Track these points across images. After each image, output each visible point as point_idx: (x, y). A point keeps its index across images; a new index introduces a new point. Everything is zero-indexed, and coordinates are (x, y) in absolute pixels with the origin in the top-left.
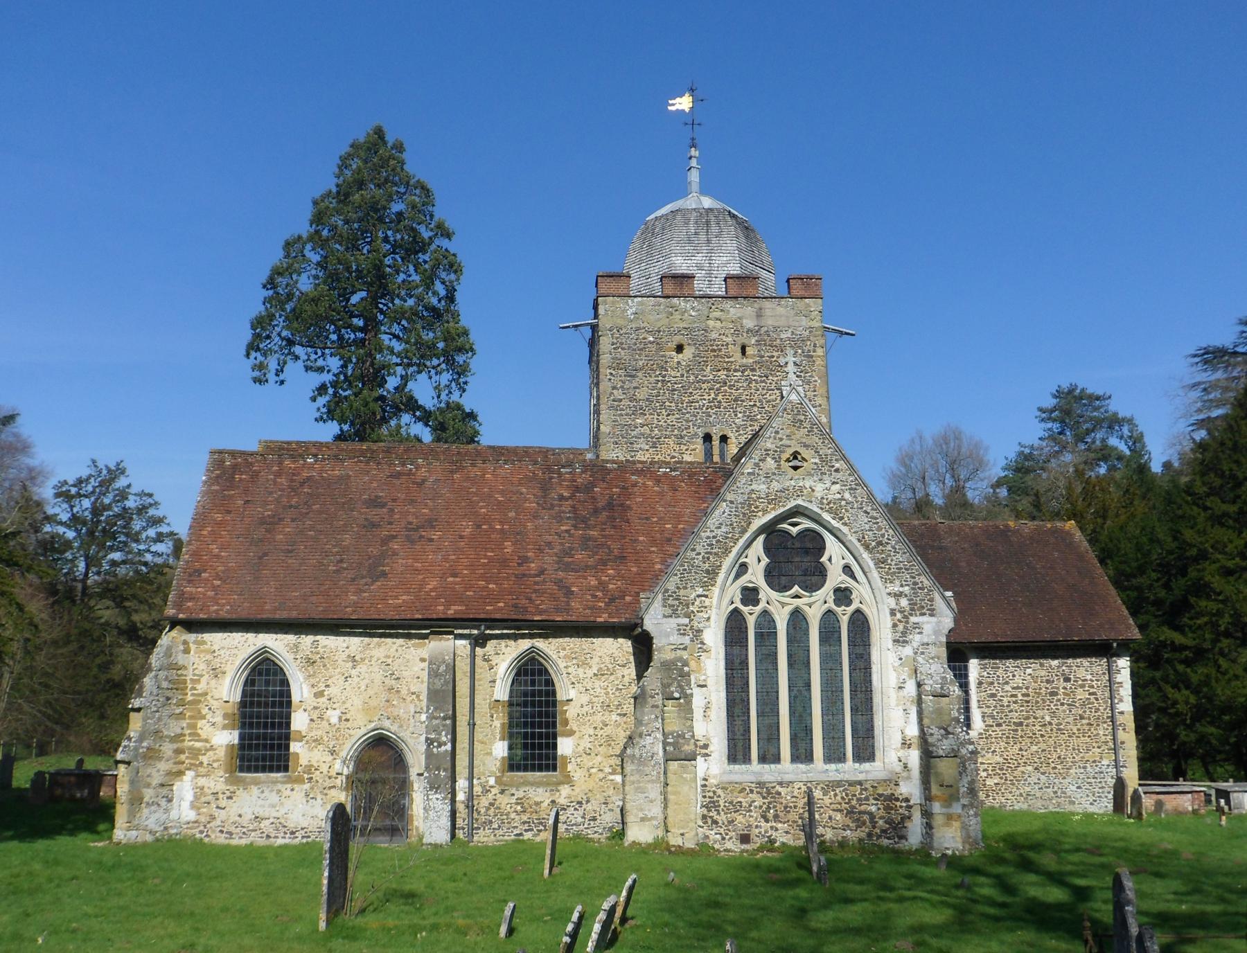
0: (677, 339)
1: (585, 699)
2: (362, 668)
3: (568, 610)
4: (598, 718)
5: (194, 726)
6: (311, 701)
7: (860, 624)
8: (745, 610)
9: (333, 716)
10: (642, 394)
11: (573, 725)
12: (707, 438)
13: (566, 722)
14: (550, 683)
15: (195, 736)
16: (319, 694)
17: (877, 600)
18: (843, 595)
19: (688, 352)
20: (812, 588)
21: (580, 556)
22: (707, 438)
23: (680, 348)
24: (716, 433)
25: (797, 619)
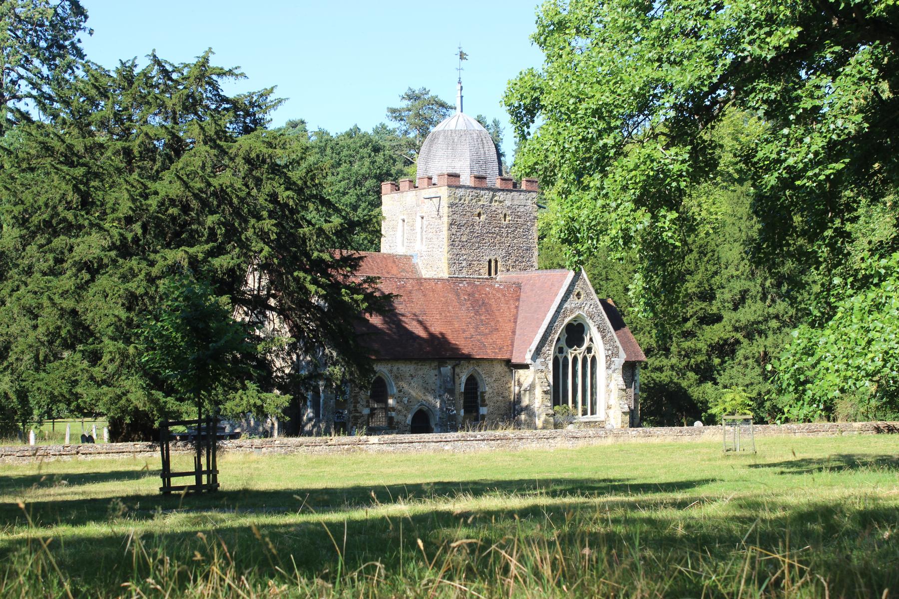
0: (478, 210)
1: (491, 391)
2: (415, 379)
3: (487, 354)
4: (495, 399)
5: (355, 407)
6: (397, 394)
7: (594, 359)
8: (559, 355)
9: (405, 400)
10: (464, 239)
11: (487, 402)
12: (490, 262)
13: (483, 400)
14: (476, 384)
15: (356, 411)
16: (400, 391)
17: (600, 350)
18: (589, 350)
19: (483, 217)
20: (580, 346)
21: (482, 328)
22: (490, 262)
23: (479, 215)
24: (493, 259)
25: (575, 359)
